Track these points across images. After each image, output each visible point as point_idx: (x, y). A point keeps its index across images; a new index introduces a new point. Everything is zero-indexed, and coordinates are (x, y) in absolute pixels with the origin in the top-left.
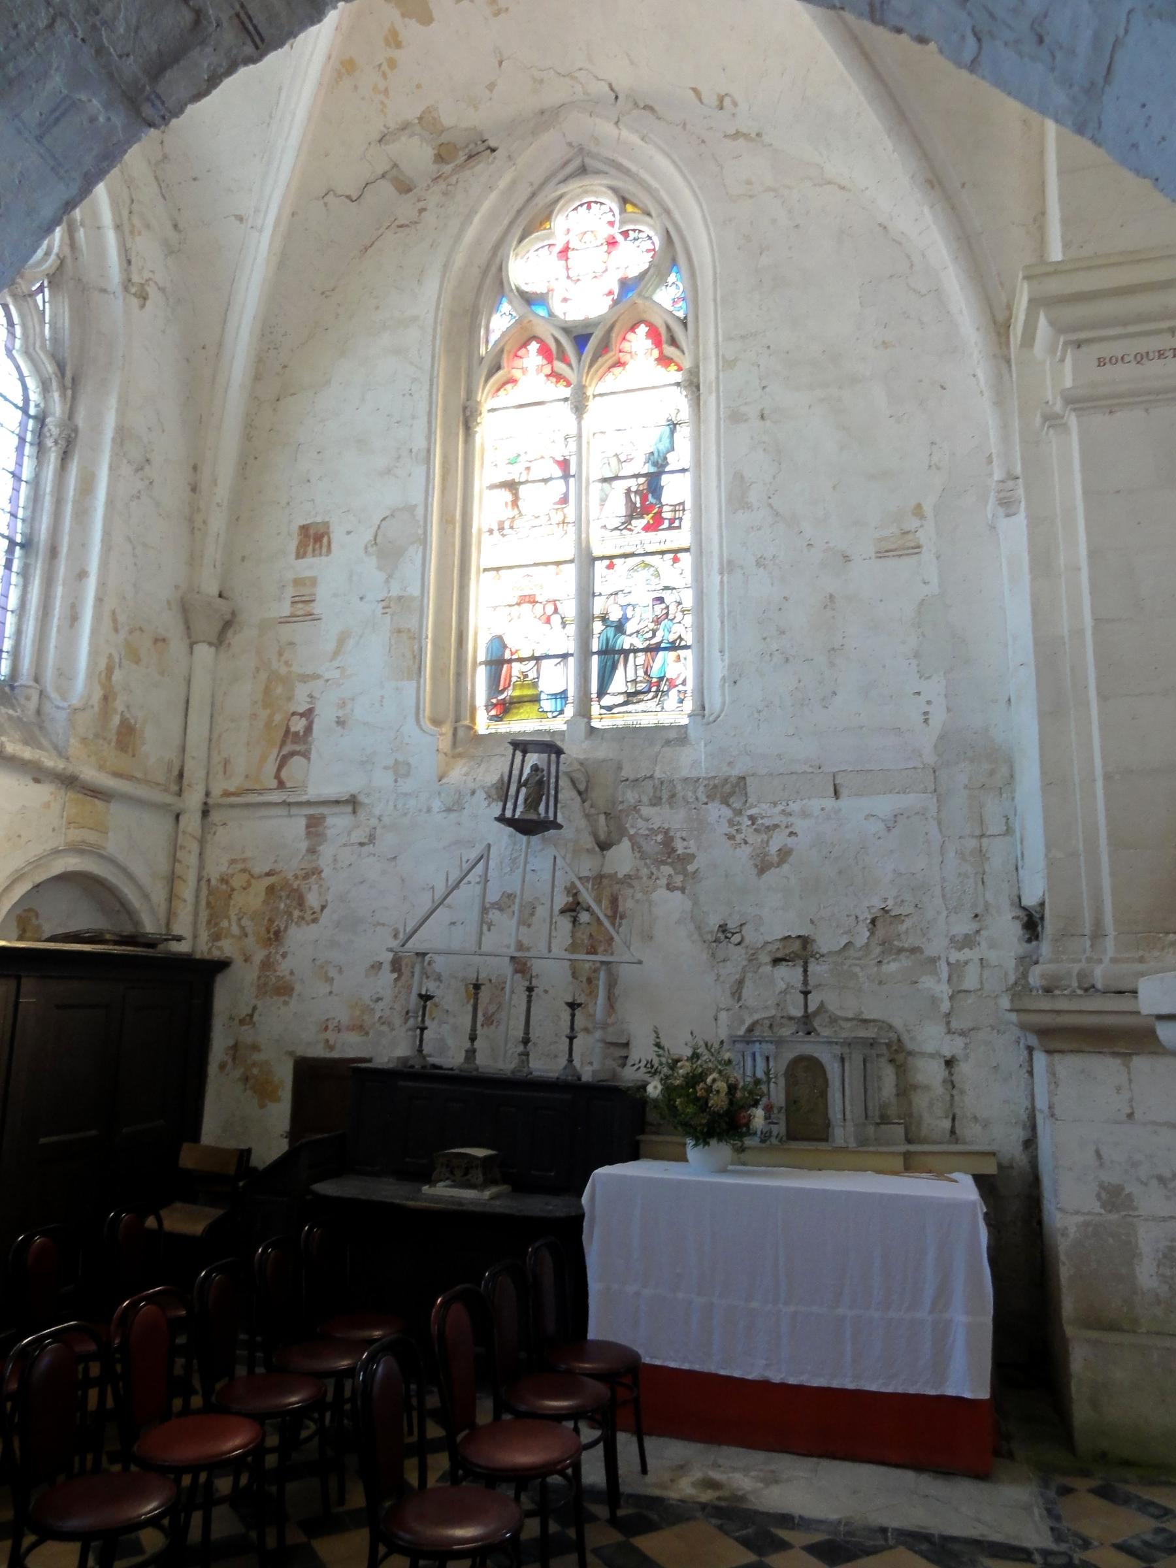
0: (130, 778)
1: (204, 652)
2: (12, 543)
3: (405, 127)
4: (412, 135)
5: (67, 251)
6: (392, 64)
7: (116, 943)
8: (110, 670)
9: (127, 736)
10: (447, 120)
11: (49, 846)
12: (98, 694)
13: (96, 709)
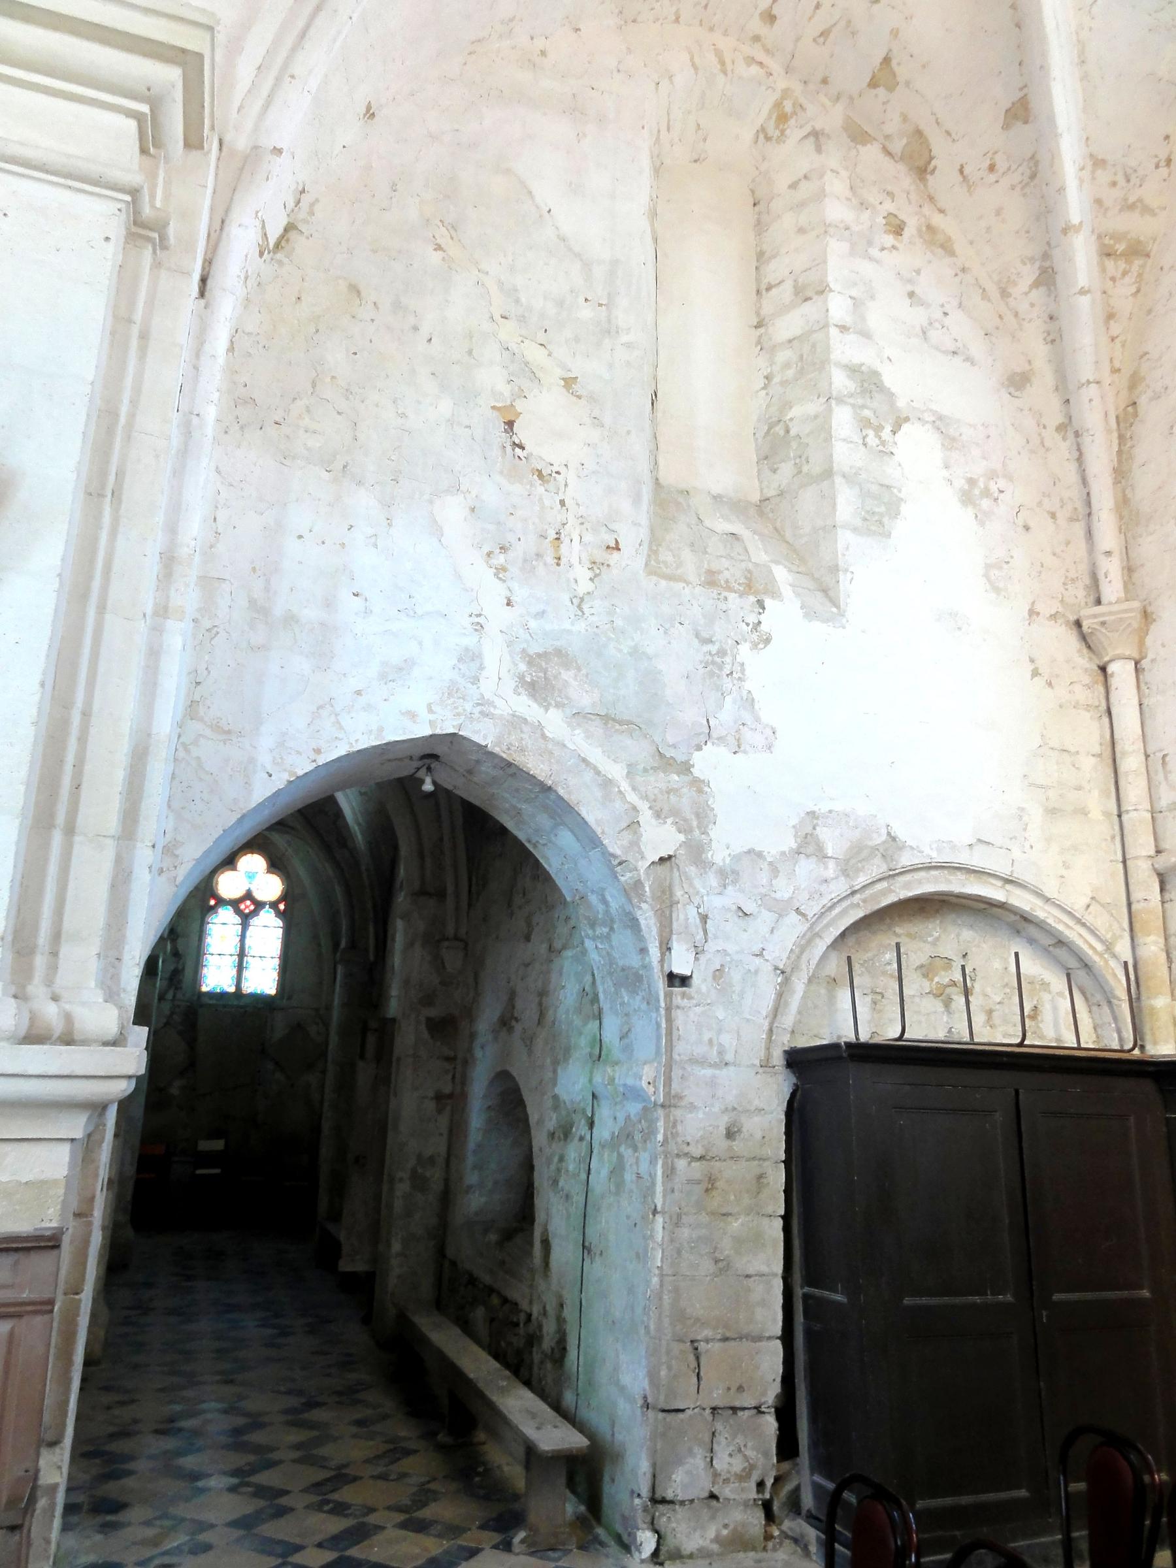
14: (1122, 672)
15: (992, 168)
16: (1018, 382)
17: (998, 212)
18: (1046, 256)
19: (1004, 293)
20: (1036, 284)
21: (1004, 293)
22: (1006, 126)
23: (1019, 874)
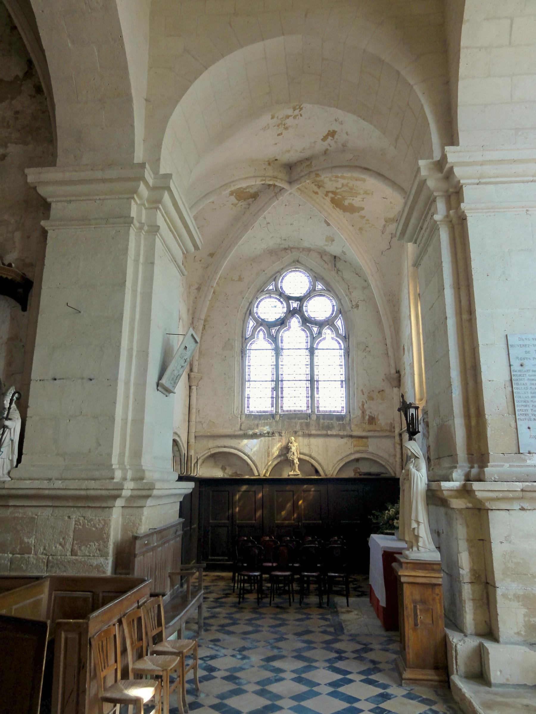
0: (375, 431)
1: (395, 390)
3: (384, 226)
4: (388, 226)
5: (341, 307)
6: (368, 220)
7: (364, 475)
8: (363, 405)
9: (372, 420)
10: (391, 215)
11: (348, 453)
12: (360, 413)
13: (360, 416)
14: (194, 388)
15: (201, 261)
16: (188, 310)
17: (197, 270)
18: (201, 284)
19: (190, 287)
20: (196, 289)
21: (190, 287)
22: (208, 255)
23: (181, 435)
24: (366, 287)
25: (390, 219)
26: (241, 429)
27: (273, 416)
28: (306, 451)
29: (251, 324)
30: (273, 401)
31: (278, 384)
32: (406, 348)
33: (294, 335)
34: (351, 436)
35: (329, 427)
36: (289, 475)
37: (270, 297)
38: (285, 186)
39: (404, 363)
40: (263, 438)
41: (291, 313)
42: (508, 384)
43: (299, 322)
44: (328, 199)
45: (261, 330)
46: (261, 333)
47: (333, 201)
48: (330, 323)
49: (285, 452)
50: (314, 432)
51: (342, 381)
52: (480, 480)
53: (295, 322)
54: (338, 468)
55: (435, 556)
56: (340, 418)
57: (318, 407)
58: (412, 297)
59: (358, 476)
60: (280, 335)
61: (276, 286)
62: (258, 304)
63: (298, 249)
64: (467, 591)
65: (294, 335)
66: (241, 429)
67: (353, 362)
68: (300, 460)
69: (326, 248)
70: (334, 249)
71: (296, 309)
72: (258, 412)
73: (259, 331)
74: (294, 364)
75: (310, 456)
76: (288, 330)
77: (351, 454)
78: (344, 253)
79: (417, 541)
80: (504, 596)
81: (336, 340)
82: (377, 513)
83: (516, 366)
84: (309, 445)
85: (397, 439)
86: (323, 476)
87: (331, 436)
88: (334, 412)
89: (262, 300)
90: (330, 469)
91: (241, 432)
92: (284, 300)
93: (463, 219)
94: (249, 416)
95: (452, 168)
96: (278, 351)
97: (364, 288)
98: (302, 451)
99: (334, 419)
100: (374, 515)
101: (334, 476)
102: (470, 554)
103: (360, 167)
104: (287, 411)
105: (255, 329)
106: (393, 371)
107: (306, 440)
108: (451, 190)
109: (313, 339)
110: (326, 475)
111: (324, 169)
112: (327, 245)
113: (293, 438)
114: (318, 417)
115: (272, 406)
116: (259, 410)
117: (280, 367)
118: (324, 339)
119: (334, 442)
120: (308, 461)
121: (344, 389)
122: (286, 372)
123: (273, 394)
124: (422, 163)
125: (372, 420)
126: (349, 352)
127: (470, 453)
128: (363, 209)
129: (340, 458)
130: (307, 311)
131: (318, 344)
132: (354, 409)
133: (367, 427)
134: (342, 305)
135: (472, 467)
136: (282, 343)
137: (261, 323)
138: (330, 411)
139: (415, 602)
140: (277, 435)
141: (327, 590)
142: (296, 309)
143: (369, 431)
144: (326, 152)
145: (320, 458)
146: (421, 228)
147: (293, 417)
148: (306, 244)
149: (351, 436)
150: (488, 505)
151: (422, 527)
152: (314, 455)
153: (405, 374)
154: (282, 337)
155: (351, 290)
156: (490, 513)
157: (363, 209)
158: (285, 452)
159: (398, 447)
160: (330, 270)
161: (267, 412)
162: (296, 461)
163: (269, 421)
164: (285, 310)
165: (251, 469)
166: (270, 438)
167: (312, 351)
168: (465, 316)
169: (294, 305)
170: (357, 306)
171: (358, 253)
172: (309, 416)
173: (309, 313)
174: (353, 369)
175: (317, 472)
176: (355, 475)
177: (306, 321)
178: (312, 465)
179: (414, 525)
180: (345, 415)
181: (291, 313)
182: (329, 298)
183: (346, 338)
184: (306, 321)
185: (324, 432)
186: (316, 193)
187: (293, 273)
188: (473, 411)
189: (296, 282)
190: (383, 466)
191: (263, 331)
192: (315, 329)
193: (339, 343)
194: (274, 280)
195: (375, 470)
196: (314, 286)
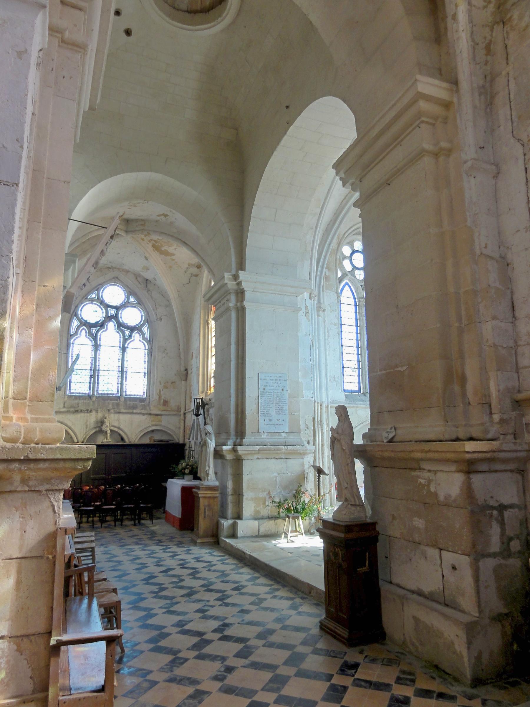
0: (167, 411)
1: (183, 382)
2: (145, 373)
3: (187, 268)
8: (160, 392)
9: (166, 403)
12: (158, 397)
24: (168, 305)
25: (192, 264)
26: (64, 407)
27: (90, 397)
28: (116, 424)
29: (75, 323)
30: (90, 386)
31: (94, 373)
32: (194, 355)
33: (110, 336)
34: (150, 414)
35: (134, 407)
36: (102, 442)
37: (93, 303)
38: (123, 233)
39: (192, 365)
40: (82, 414)
41: (108, 318)
42: (257, 398)
43: (115, 326)
44: (151, 244)
45: (83, 329)
46: (84, 331)
47: (154, 246)
48: (139, 329)
49: (99, 425)
50: (123, 411)
51: (145, 373)
52: (240, 445)
53: (111, 325)
54: (139, 437)
55: (217, 484)
56: (142, 400)
57: (125, 392)
58: (202, 322)
59: (152, 442)
60: (99, 334)
61: (98, 295)
62: (82, 308)
63: (119, 269)
64: (230, 499)
65: (110, 336)
66: (64, 407)
67: (154, 360)
68: (111, 430)
69: (141, 273)
70: (148, 275)
71: (113, 315)
72: (77, 393)
73: (82, 330)
74: (109, 357)
75: (119, 428)
76: (105, 331)
77: (149, 427)
78: (155, 279)
79: (208, 477)
80: (247, 499)
81: (143, 342)
82: (174, 466)
83: (261, 389)
84: (118, 420)
85: (182, 416)
86: (127, 442)
87: (136, 413)
88: (138, 395)
89: (85, 305)
90: (133, 437)
91: (65, 410)
92: (104, 307)
93: (243, 309)
94: (70, 397)
95: (241, 281)
96: (97, 347)
97: (167, 306)
98: (113, 424)
99: (138, 401)
100: (173, 467)
101: (136, 442)
102: (233, 481)
103: (181, 240)
104: (102, 394)
105: (78, 327)
106: (183, 369)
107: (117, 416)
108: (239, 291)
109: (125, 340)
110: (130, 442)
111: (154, 231)
112: (142, 272)
113: (107, 415)
114: (126, 399)
115: (90, 390)
116: (78, 392)
117: (98, 359)
118: (133, 340)
119: (137, 418)
120: (117, 432)
121: (146, 379)
122: (102, 364)
123: (90, 380)
124: (227, 275)
125: (166, 403)
126: (151, 352)
127: (237, 432)
128: (174, 255)
129: (141, 429)
130: (121, 318)
131: (128, 344)
132: (153, 394)
133: (162, 408)
134: (149, 316)
135: (237, 439)
136: (100, 340)
137: (84, 323)
138: (135, 395)
139: (205, 506)
140: (94, 412)
141: (137, 517)
142: (113, 315)
143: (163, 411)
144: (157, 221)
145: (126, 430)
146: (220, 302)
147: (106, 398)
148: (126, 268)
149: (150, 414)
150: (243, 457)
151: (211, 469)
152: (121, 427)
153: (192, 372)
154: (100, 336)
155: (157, 307)
156: (244, 462)
157: (174, 255)
158: (99, 425)
159: (182, 422)
160: (141, 289)
161: (85, 394)
162: (109, 432)
163: (87, 401)
164: (104, 315)
165: (71, 437)
166: (89, 414)
167: (124, 349)
168: (240, 361)
169: (112, 312)
170: (161, 319)
171: (167, 283)
172: (119, 398)
173: (123, 319)
174: (154, 365)
175: (122, 439)
176: (150, 441)
177: (120, 326)
178: (120, 435)
179: (207, 468)
180: (145, 398)
181: (108, 318)
182: (139, 310)
183: (150, 341)
184: (120, 326)
185: (131, 411)
186: (143, 240)
187: (112, 286)
188: (240, 410)
189: (114, 294)
190: (170, 435)
191: (85, 330)
192: (127, 333)
193: (144, 345)
194: (97, 290)
195: (165, 438)
196: (128, 299)
